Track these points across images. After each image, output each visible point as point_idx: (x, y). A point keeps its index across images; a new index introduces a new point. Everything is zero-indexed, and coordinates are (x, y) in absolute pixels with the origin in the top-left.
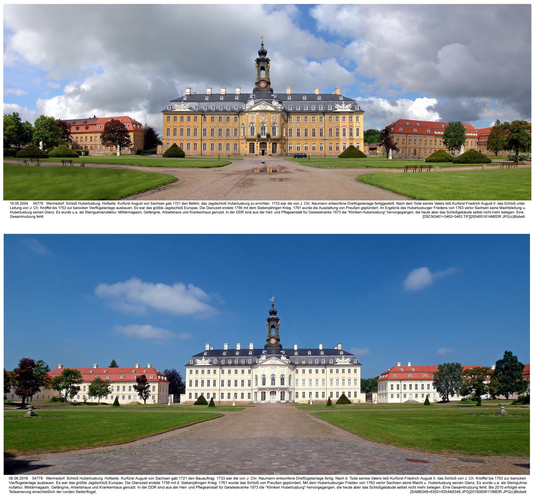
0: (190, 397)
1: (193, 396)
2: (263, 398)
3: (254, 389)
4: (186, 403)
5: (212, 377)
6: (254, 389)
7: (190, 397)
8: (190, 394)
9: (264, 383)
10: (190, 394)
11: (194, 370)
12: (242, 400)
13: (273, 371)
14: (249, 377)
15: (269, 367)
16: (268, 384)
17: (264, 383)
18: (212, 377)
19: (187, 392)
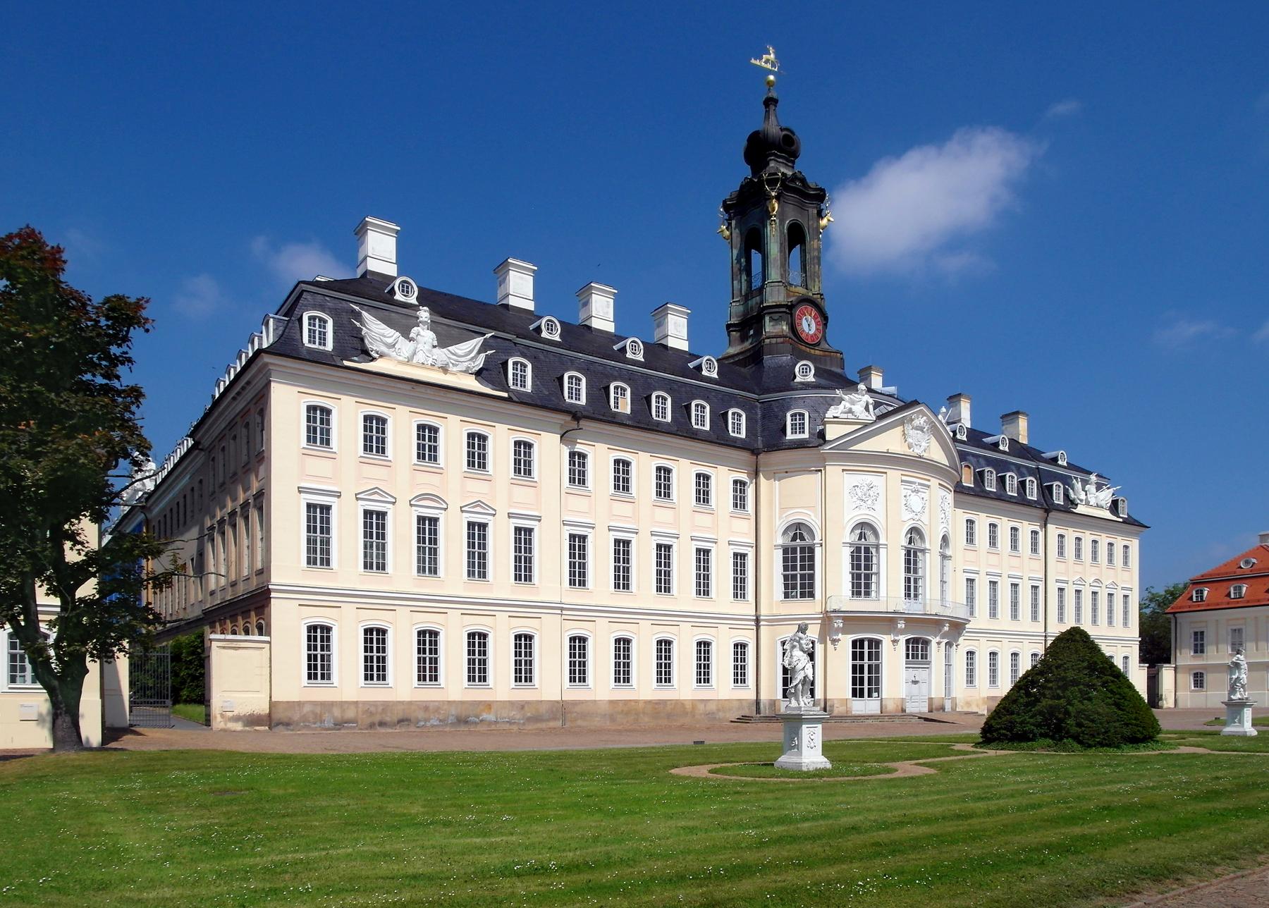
0: (318, 667)
1: (347, 654)
2: (865, 679)
3: (775, 621)
4: (272, 719)
5: (502, 496)
6: (775, 621)
7: (318, 667)
8: (319, 636)
9: (862, 582)
10: (319, 636)
11: (348, 414)
12: (703, 693)
13: (915, 502)
14: (742, 530)
15: (895, 475)
16: (889, 591)
17: (862, 582)
18: (502, 496)
19: (288, 620)
